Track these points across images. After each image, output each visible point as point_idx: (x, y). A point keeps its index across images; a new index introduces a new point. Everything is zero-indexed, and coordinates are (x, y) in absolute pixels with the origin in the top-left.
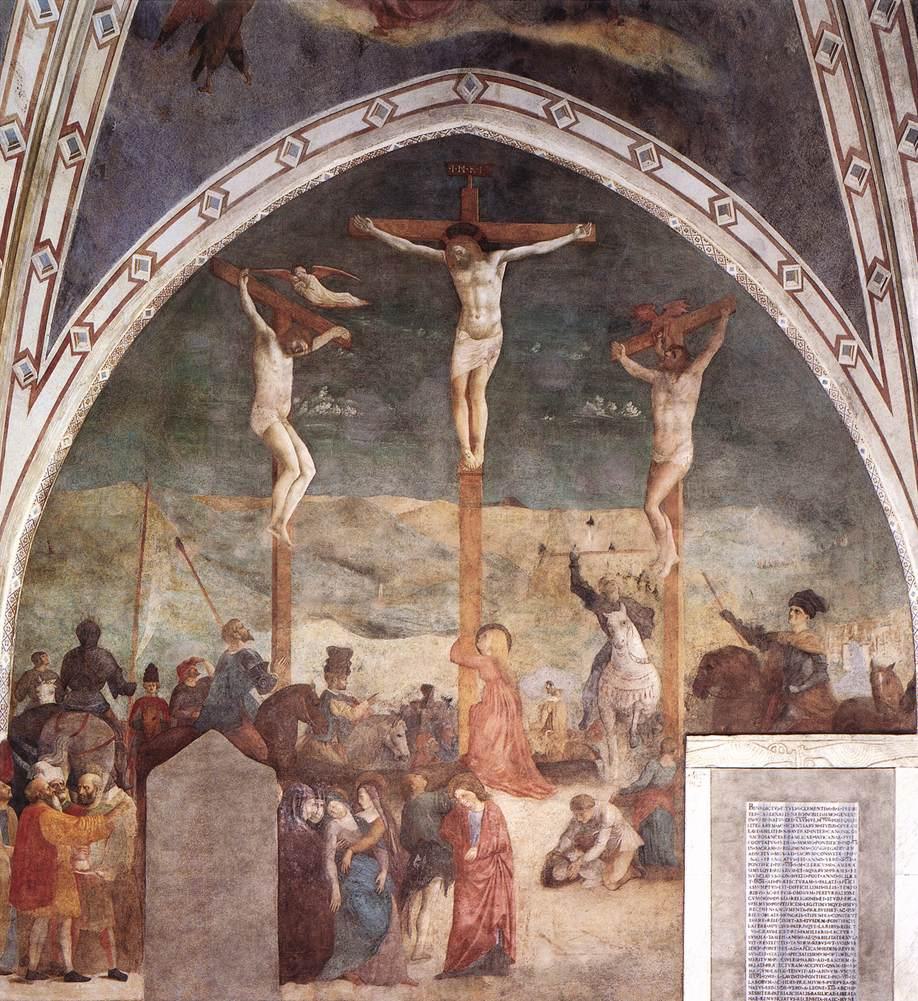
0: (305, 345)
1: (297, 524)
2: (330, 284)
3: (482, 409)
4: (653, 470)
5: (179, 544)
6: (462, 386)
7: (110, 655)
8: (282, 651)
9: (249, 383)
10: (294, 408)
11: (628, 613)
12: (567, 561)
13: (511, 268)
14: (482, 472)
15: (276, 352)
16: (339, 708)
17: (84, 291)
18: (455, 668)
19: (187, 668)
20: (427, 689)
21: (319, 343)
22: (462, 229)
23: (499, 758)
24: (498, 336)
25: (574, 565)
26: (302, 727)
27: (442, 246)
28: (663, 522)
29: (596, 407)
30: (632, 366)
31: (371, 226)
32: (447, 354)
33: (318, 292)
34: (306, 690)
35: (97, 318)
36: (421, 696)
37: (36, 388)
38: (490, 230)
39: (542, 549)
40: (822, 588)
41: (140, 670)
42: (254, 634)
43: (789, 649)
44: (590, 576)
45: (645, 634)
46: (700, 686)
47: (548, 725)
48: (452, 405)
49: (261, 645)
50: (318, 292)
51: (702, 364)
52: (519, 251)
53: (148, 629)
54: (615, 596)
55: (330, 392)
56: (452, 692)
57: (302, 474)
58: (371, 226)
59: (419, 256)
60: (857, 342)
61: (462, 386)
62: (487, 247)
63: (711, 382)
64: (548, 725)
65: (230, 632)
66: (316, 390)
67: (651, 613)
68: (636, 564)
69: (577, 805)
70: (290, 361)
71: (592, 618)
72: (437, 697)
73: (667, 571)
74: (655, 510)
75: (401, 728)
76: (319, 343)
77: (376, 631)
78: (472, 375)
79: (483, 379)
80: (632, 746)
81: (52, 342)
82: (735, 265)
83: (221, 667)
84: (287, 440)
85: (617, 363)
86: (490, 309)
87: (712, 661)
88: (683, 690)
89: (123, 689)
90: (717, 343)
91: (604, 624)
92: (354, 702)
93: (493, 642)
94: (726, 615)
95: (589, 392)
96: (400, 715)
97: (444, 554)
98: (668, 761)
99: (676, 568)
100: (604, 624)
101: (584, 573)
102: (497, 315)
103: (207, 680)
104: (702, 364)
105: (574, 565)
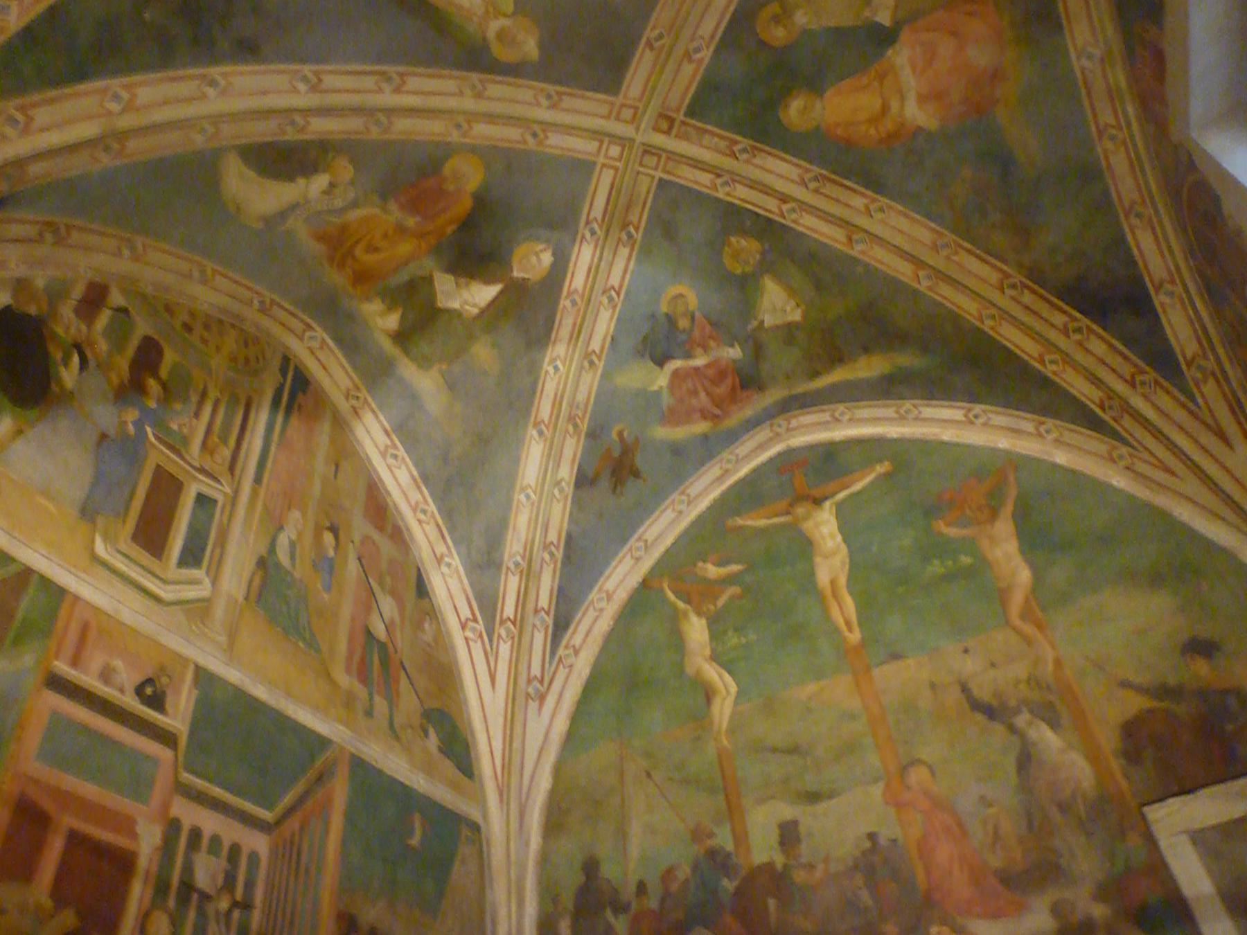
0: (712, 607)
1: (731, 731)
2: (720, 564)
3: (849, 603)
4: (1003, 596)
5: (649, 775)
6: (828, 592)
7: (609, 881)
8: (741, 838)
9: (678, 642)
10: (713, 650)
11: (1031, 712)
12: (957, 689)
13: (840, 509)
14: (863, 644)
16: (800, 876)
17: (566, 627)
18: (892, 811)
19: (668, 874)
20: (872, 836)
21: (721, 602)
22: (800, 498)
23: (960, 886)
24: (844, 550)
25: (965, 689)
26: (772, 903)
27: (788, 513)
28: (1028, 629)
29: (936, 568)
30: (952, 532)
31: (740, 521)
32: (811, 574)
33: (712, 571)
34: (769, 867)
35: (577, 640)
36: (868, 844)
38: (816, 492)
39: (933, 686)
40: (1206, 631)
41: (632, 888)
42: (715, 830)
43: (1202, 694)
44: (983, 693)
45: (1054, 725)
46: (1131, 756)
47: (996, 835)
49: (724, 839)
50: (712, 571)
51: (1008, 509)
52: (841, 496)
53: (634, 851)
54: (1013, 703)
55: (736, 630)
56: (896, 832)
57: (728, 692)
58: (740, 521)
59: (774, 526)
60: (1124, 450)
61: (828, 592)
62: (818, 502)
63: (1022, 518)
64: (996, 835)
65: (698, 834)
66: (725, 632)
67: (1050, 706)
68: (1020, 670)
70: (704, 622)
71: (999, 728)
72: (883, 841)
73: (1050, 667)
74: (1017, 622)
75: (859, 879)
76: (721, 602)
77: (813, 797)
79: (842, 581)
80: (1089, 834)
81: (550, 663)
83: (695, 867)
84: (713, 673)
85: (940, 534)
86: (833, 537)
87: (1131, 730)
88: (1116, 765)
89: (620, 908)
90: (1013, 492)
91: (1012, 729)
92: (811, 867)
93: (918, 776)
94: (1125, 684)
95: (926, 560)
96: (856, 867)
97: (852, 717)
98: (1134, 840)
99: (1058, 663)
100: (1012, 729)
101: (976, 692)
102: (839, 538)
103: (687, 881)
104: (1008, 509)
105: (965, 689)
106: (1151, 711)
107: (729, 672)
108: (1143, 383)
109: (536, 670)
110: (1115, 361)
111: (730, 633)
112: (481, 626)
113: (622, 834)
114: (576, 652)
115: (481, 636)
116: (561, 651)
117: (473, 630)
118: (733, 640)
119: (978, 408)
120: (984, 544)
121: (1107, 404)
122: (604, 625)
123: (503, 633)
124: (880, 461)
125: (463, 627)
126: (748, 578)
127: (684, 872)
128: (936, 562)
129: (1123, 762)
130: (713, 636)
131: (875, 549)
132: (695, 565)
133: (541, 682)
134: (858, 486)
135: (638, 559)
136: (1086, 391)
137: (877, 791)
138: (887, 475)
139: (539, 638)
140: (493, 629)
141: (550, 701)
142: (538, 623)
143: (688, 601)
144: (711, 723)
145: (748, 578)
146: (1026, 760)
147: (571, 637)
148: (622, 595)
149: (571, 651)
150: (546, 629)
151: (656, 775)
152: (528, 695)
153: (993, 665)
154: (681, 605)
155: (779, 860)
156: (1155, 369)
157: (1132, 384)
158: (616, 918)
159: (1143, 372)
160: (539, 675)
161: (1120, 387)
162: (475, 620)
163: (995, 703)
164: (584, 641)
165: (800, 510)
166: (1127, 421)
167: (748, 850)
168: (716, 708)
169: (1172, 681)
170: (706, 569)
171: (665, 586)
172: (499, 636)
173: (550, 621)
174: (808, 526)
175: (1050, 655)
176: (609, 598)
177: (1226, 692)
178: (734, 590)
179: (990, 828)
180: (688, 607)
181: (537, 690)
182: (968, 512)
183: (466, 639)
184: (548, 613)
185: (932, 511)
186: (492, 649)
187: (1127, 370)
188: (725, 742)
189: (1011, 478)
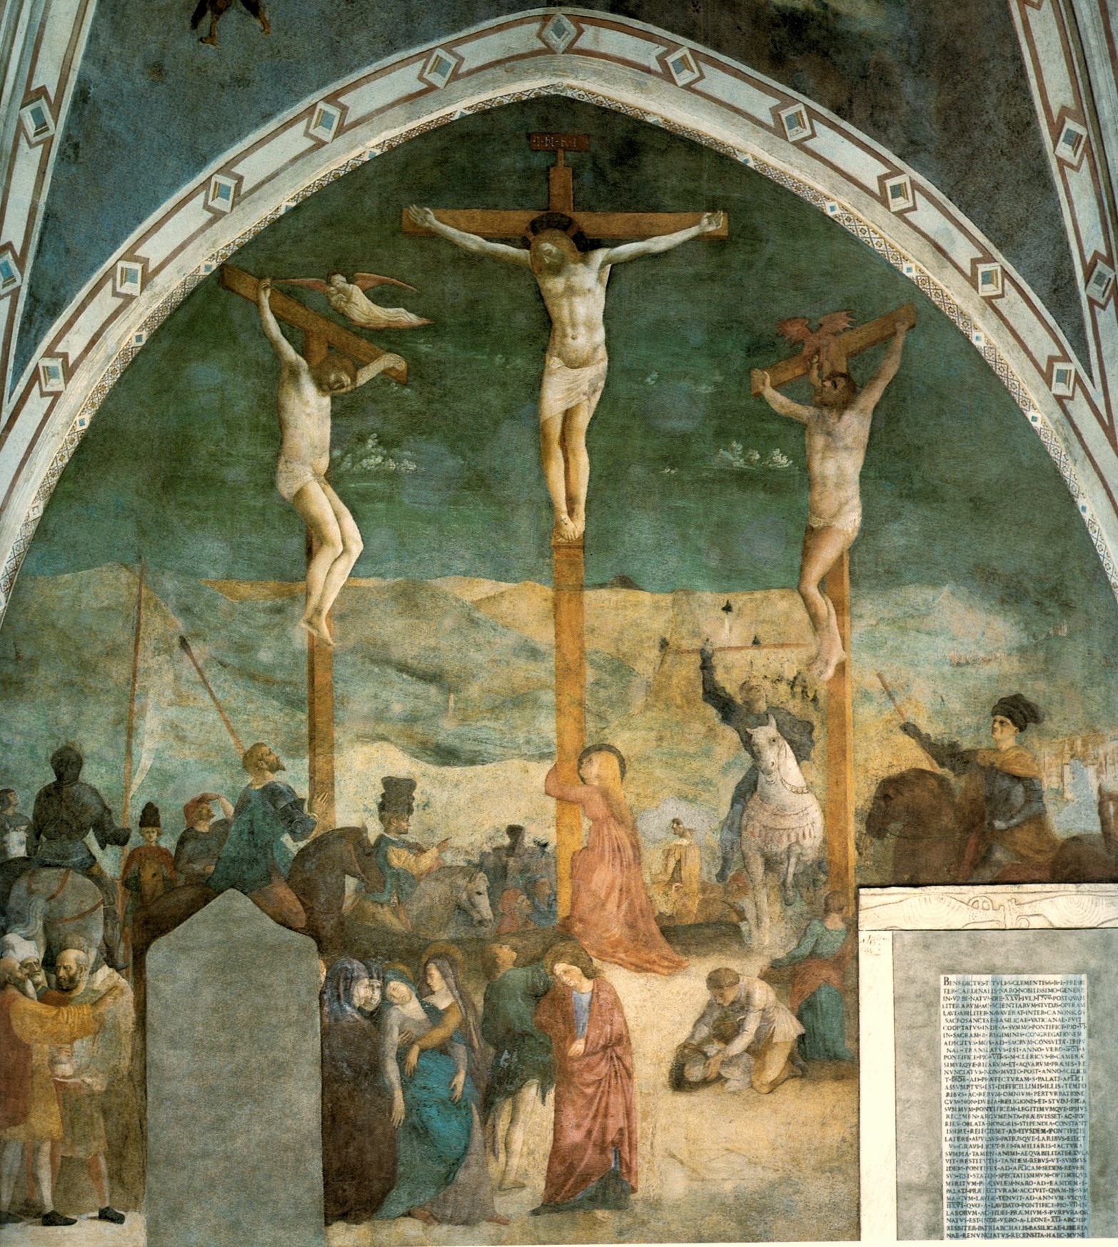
0: (346, 379)
1: (339, 616)
2: (378, 297)
3: (582, 461)
4: (810, 536)
5: (184, 643)
6: (555, 430)
7: (95, 792)
8: (323, 784)
10: (334, 464)
11: (779, 728)
12: (697, 659)
13: (616, 275)
14: (583, 544)
15: (309, 389)
16: (399, 858)
17: (54, 310)
18: (551, 804)
20: (515, 831)
21: (365, 376)
22: (551, 222)
24: (600, 367)
25: (706, 665)
26: (351, 883)
27: (526, 244)
28: (824, 606)
29: (733, 456)
30: (779, 401)
31: (432, 219)
32: (535, 387)
33: (362, 308)
34: (356, 835)
35: (74, 344)
36: (507, 841)
38: (589, 222)
39: (664, 644)
40: (1035, 691)
41: (136, 812)
42: (285, 762)
43: (992, 772)
44: (728, 682)
45: (801, 754)
46: (875, 823)
48: (542, 457)
50: (362, 308)
51: (871, 398)
53: (145, 759)
55: (381, 442)
56: (550, 835)
57: (346, 550)
58: (432, 219)
59: (495, 258)
60: (1075, 366)
61: (555, 430)
62: (586, 245)
65: (253, 760)
66: (362, 439)
67: (809, 727)
68: (789, 663)
69: (715, 981)
70: (327, 401)
71: (730, 735)
72: (528, 841)
73: (830, 672)
74: (813, 590)
75: (482, 882)
76: (365, 376)
77: (446, 755)
79: (583, 420)
80: (787, 903)
85: (759, 396)
86: (590, 327)
87: (890, 789)
88: (853, 828)
90: (891, 368)
91: (748, 742)
92: (419, 850)
93: (600, 768)
94: (909, 729)
95: (722, 435)
97: (534, 653)
98: (835, 923)
99: (841, 668)
100: (748, 742)
101: (720, 676)
102: (600, 335)
103: (225, 823)
104: (871, 398)
105: (706, 665)
106: (921, 773)
107: (353, 512)
113: (127, 727)
114: (69, 372)
116: (37, 359)
126: (424, 348)
127: (224, 809)
128: (738, 447)
129: (863, 828)
134: (659, 244)
135: (217, 216)
137: (540, 772)
138: (715, 244)
144: (308, 594)
145: (424, 348)
146: (748, 789)
148: (171, 283)
149: (57, 363)
151: (196, 648)
153: (756, 642)
154: (290, 352)
155: (374, 829)
158: (103, 848)
167: (331, 801)
169: (966, 744)
171: (265, 299)
175: (836, 656)
177: (1018, 779)
178: (390, 361)
179: (672, 864)
182: (815, 373)
189: (899, 342)
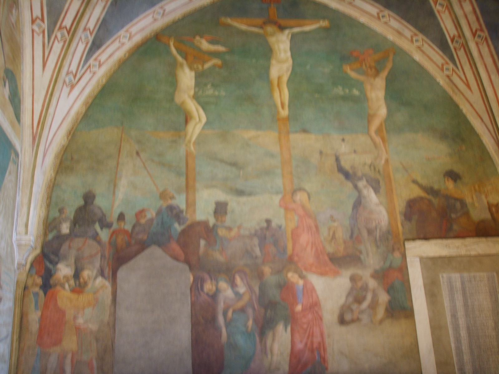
1: (197, 143)
2: (212, 42)
4: (370, 118)
5: (138, 153)
6: (275, 82)
7: (100, 208)
8: (190, 204)
9: (174, 82)
10: (195, 93)
11: (367, 181)
12: (333, 159)
13: (293, 37)
14: (288, 118)
15: (187, 70)
16: (222, 232)
18: (282, 211)
19: (140, 213)
20: (268, 222)
21: (207, 65)
22: (270, 21)
23: (309, 256)
24: (290, 62)
25: (337, 159)
26: (202, 243)
27: (261, 27)
28: (378, 140)
29: (339, 91)
30: (353, 75)
32: (267, 69)
33: (205, 45)
34: (205, 224)
35: (103, 58)
36: (265, 225)
37: (72, 87)
38: (282, 22)
39: (321, 153)
40: (457, 168)
41: (115, 215)
42: (175, 195)
43: (447, 197)
44: (346, 164)
45: (376, 191)
46: (408, 216)
47: (334, 237)
48: (271, 91)
49: (180, 201)
50: (205, 45)
51: (384, 74)
52: (296, 30)
53: (120, 194)
54: (359, 174)
55: (213, 85)
56: (283, 222)
57: (200, 120)
58: (229, 21)
59: (252, 33)
60: (451, 66)
61: (275, 82)
62: (282, 28)
63: (390, 81)
64: (334, 237)
65: (163, 195)
66: (206, 85)
67: (378, 182)
68: (368, 159)
69: (353, 279)
70: (193, 74)
71: (349, 185)
72: (274, 225)
73: (383, 162)
74: (373, 134)
75: (256, 241)
76: (207, 65)
77: (240, 193)
78: (279, 78)
79: (285, 79)
80: (378, 247)
81: (83, 67)
82: (391, 37)
83: (159, 212)
84: (192, 106)
85: (346, 73)
86: (285, 51)
87: (411, 204)
88: (399, 218)
89: (105, 224)
90: (389, 65)
91: (356, 187)
92: (230, 229)
93: (300, 197)
94: (415, 182)
95: (335, 84)
96: (256, 234)
97: (272, 156)
98: (397, 255)
99: (387, 161)
100: (356, 187)
101: (343, 163)
102: (289, 54)
103: (152, 220)
104: (384, 74)
105: (337, 159)
106: (422, 198)
107: (204, 109)
108: (479, 36)
109: (73, 68)
110: (472, 18)
111: (209, 86)
112: (45, 26)
113: (114, 184)
114: (100, 65)
115: (44, 32)
116: (91, 61)
117: (40, 27)
118: (210, 91)
119: (387, 12)
120: (368, 87)
121: (456, 39)
122: (120, 54)
123: (59, 36)
124: (324, 18)
125: (33, 22)
126: (227, 57)
127: (151, 214)
128: (340, 88)
129: (403, 218)
130: (197, 85)
131: (308, 67)
132: (194, 37)
133: (75, 76)
134: (307, 28)
135: (155, 20)
136: (449, 28)
137: (277, 199)
138: (326, 29)
139: (81, 47)
140: (53, 31)
141: (76, 91)
142: (83, 38)
143: (186, 58)
144: (186, 135)
145: (227, 57)
146: (358, 204)
147: (98, 56)
149: (97, 63)
150: (87, 44)
151: (142, 155)
152: (64, 82)
153: (355, 152)
154: (180, 59)
155: (212, 221)
156: (489, 32)
157: (474, 35)
158: (102, 228)
159: (482, 30)
160: (74, 72)
161: (468, 34)
162: (43, 20)
163: (351, 172)
164: (107, 59)
165: (270, 29)
166: (461, 53)
167: (194, 211)
168: (190, 127)
169: (436, 187)
170: (201, 43)
171: (172, 44)
172: (56, 37)
173: (91, 39)
174: (272, 40)
175: (384, 157)
176: (130, 38)
177: (456, 199)
178: (216, 61)
179: (331, 233)
180: (184, 62)
181: (70, 81)
182: (364, 67)
183: (33, 31)
184: (91, 34)
185: (345, 58)
186: (49, 42)
187: (475, 26)
188: (192, 148)
189: (391, 57)
